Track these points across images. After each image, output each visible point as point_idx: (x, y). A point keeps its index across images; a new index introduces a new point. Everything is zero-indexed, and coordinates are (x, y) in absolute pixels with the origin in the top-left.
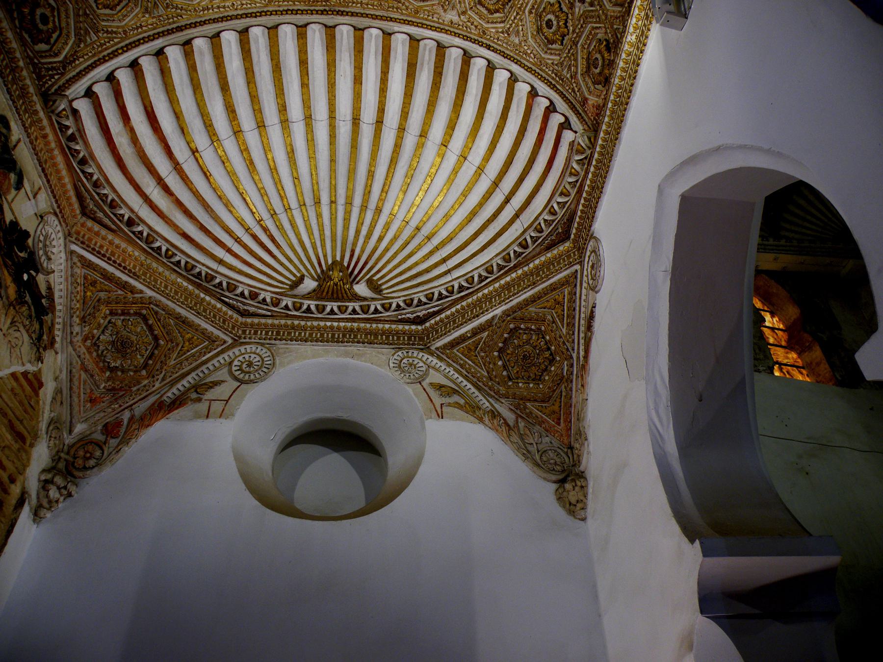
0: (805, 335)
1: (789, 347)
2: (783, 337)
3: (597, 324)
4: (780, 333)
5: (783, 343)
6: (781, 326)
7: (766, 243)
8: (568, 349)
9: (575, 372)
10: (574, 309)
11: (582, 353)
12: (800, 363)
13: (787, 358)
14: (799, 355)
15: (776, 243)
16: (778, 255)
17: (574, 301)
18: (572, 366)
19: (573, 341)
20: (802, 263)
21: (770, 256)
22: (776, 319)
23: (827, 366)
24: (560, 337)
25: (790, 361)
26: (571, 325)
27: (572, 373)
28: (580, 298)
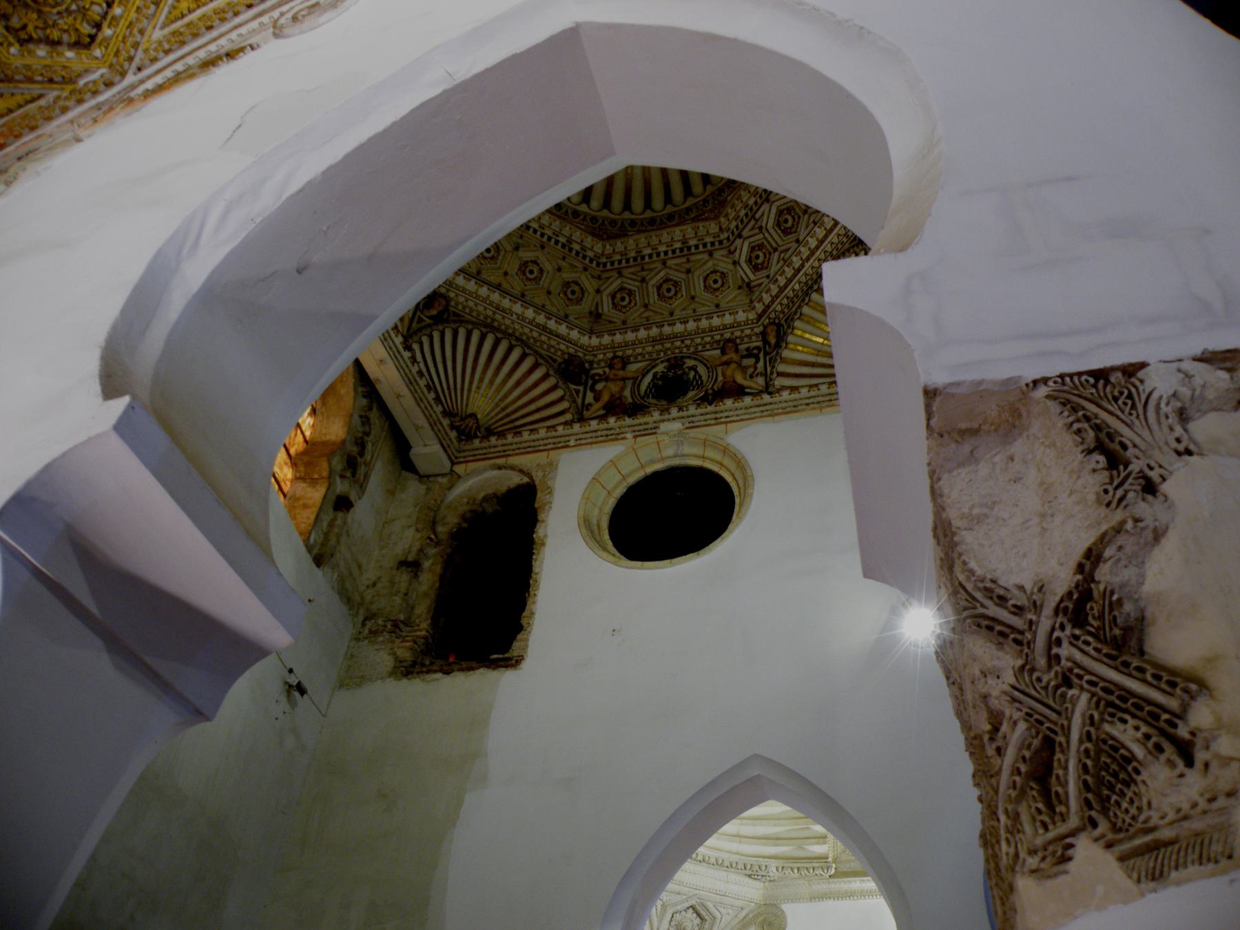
0: (325, 465)
1: (293, 461)
2: (297, 445)
3: (225, 70)
4: (300, 438)
5: (292, 451)
6: (308, 434)
7: (393, 335)
8: (131, 59)
9: (101, 98)
10: (210, 28)
11: (149, 85)
12: (286, 488)
13: (281, 469)
14: (297, 479)
15: (400, 347)
16: (389, 360)
17: (223, 20)
18: (109, 84)
19: (154, 60)
20: (399, 396)
21: (382, 352)
22: (310, 421)
23: (313, 517)
24: (142, 32)
25: (280, 476)
26: (179, 39)
27: (95, 93)
28: (236, 27)
